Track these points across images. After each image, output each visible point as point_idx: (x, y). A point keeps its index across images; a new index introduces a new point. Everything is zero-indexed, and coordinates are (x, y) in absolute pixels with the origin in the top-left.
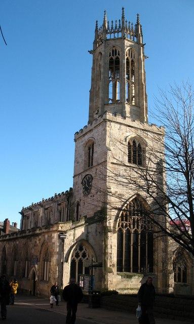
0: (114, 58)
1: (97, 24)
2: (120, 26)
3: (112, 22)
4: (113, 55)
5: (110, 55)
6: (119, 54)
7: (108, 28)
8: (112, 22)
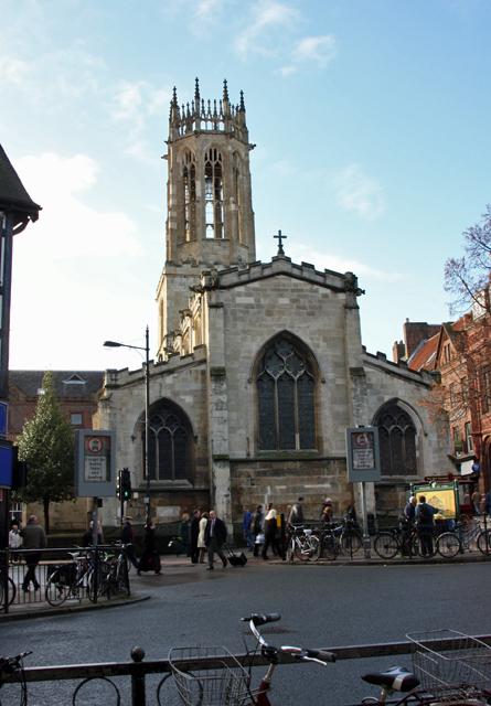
0: (213, 164)
6: (220, 159)
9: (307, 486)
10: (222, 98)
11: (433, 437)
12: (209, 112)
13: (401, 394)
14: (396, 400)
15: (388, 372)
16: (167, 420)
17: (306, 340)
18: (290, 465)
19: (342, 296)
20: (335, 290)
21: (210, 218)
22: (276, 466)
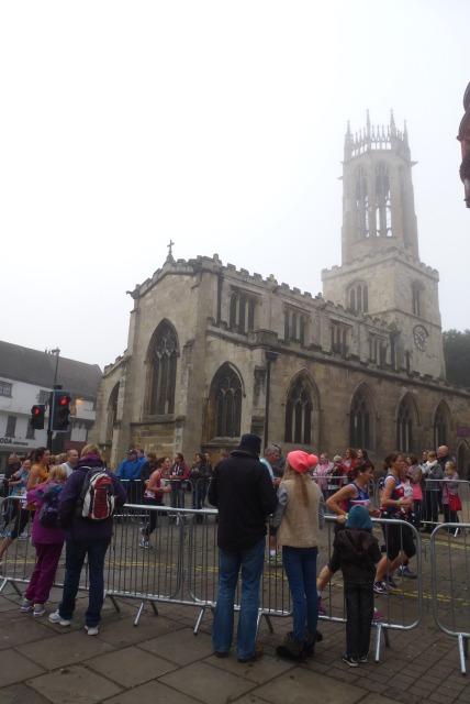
15: (224, 338)
17: (174, 322)
19: (195, 279)
20: (192, 275)
22: (152, 428)
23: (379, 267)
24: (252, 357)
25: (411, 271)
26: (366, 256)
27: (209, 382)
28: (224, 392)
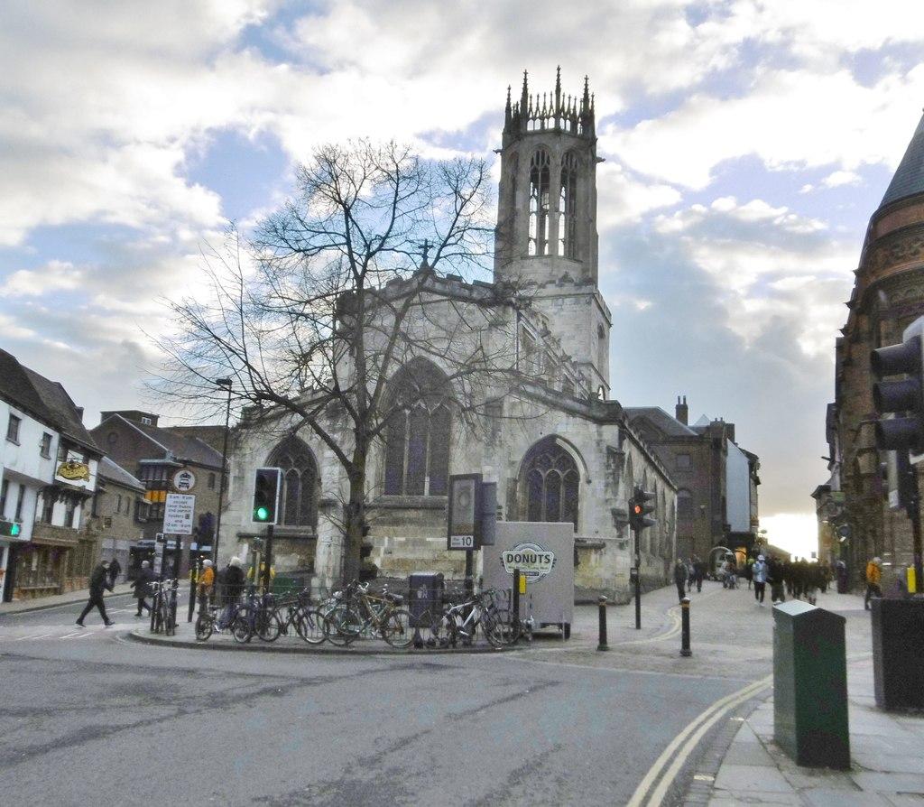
0: (540, 168)
1: (509, 99)
2: (551, 107)
3: (538, 96)
4: (538, 164)
5: (532, 163)
7: (531, 109)
8: (538, 96)
9: (428, 539)
10: (554, 89)
11: (599, 483)
12: (538, 109)
13: (560, 430)
14: (553, 437)
16: (297, 461)
18: (412, 514)
21: (533, 232)
23: (567, 300)
24: (600, 434)
25: (599, 312)
26: (547, 283)
27: (519, 457)
28: (544, 475)
